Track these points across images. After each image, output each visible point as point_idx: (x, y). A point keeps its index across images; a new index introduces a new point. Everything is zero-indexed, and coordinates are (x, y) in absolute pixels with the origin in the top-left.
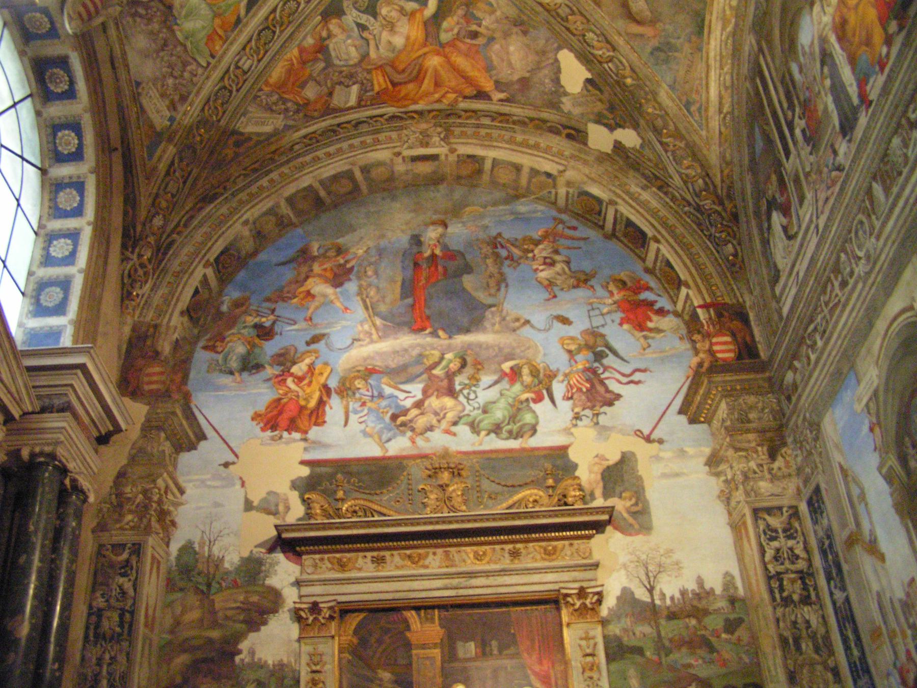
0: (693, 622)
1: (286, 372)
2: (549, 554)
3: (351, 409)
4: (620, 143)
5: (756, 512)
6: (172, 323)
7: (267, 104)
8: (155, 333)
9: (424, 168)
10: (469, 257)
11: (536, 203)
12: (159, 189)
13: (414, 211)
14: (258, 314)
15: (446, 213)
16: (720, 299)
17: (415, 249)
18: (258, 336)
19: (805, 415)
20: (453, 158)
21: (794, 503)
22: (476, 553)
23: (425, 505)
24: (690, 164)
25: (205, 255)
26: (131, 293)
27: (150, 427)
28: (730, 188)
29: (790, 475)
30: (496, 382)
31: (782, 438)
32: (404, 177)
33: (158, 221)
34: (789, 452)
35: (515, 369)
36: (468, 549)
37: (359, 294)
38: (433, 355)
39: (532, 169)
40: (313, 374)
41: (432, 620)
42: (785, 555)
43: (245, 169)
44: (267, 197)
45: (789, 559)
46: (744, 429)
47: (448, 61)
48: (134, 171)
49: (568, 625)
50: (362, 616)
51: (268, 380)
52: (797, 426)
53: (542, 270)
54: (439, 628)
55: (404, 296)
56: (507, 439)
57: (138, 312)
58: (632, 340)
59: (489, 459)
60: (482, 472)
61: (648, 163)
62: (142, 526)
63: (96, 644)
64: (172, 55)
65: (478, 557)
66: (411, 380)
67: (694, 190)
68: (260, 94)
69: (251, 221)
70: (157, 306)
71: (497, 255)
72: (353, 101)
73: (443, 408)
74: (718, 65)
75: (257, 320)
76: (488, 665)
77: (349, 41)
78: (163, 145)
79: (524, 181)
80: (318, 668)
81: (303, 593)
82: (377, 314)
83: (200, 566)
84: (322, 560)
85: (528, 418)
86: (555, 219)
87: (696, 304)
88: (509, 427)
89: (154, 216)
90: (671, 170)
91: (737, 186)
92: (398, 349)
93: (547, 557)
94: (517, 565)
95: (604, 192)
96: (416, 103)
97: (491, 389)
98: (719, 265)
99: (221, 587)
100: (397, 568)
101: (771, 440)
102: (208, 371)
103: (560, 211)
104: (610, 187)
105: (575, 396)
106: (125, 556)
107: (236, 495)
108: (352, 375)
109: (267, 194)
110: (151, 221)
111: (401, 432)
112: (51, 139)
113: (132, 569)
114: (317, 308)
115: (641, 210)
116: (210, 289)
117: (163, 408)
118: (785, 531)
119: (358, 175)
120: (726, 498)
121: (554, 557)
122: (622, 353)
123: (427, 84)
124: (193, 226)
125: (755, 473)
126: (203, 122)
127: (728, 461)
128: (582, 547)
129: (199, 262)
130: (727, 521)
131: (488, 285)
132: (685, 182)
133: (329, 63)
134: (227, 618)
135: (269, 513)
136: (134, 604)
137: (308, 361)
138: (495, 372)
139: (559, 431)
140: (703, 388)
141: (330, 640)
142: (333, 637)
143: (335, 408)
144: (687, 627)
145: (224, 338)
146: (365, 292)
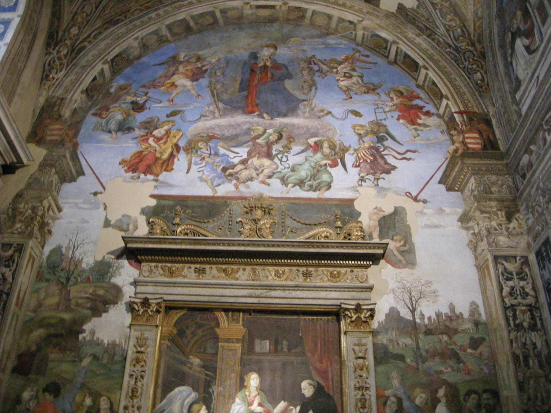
0: (446, 338)
1: (150, 134)
2: (334, 277)
3: (193, 161)
4: (403, 5)
5: (496, 258)
6: (75, 97)
8: (61, 103)
12: (78, 9)
13: (254, 38)
14: (135, 95)
16: (470, 109)
17: (253, 61)
18: (133, 109)
19: (538, 185)
20: (285, 8)
21: (525, 254)
22: (277, 271)
23: (240, 233)
24: (452, 18)
25: (105, 56)
26: (49, 76)
27: (44, 165)
28: (480, 35)
29: (522, 233)
30: (303, 151)
31: (516, 206)
33: (74, 31)
34: (521, 217)
35: (318, 143)
36: (271, 268)
37: (209, 86)
38: (258, 129)
40: (168, 137)
41: (238, 322)
42: (518, 292)
43: (141, 6)
44: (154, 24)
45: (521, 295)
46: (488, 198)
49: (345, 333)
50: (182, 313)
51: (136, 138)
52: (530, 196)
53: (342, 81)
54: (242, 327)
55: (241, 90)
56: (308, 191)
57: (52, 90)
58: (406, 130)
59: (293, 204)
60: (287, 213)
61: (422, 18)
62: (27, 232)
65: (277, 275)
66: (240, 145)
67: (454, 36)
69: (140, 37)
71: (311, 69)
75: (134, 99)
76: (279, 359)
79: (333, 24)
80: (142, 349)
81: (138, 291)
83: (64, 265)
84: (156, 267)
85: (325, 177)
86: (354, 49)
87: (453, 111)
88: (310, 183)
89: (72, 27)
90: (438, 23)
91: (486, 33)
93: (332, 279)
94: (308, 283)
95: (389, 35)
97: (299, 155)
98: (471, 88)
99: (77, 281)
100: (214, 277)
101: (508, 207)
103: (358, 45)
105: (361, 165)
106: (10, 252)
108: (197, 139)
109: (153, 22)
111: (228, 180)
113: (13, 262)
114: (178, 94)
115: (416, 49)
116: (104, 78)
118: (518, 274)
119: (218, 14)
120: (474, 248)
121: (338, 279)
122: (398, 138)
125: (496, 230)
127: (475, 220)
128: (360, 274)
130: (474, 263)
131: (303, 87)
132: (448, 31)
134: (78, 305)
135: (121, 229)
136: (10, 288)
137: (166, 127)
138: (303, 144)
139: (348, 189)
140: (458, 166)
141: (155, 329)
143: (181, 161)
144: (440, 341)
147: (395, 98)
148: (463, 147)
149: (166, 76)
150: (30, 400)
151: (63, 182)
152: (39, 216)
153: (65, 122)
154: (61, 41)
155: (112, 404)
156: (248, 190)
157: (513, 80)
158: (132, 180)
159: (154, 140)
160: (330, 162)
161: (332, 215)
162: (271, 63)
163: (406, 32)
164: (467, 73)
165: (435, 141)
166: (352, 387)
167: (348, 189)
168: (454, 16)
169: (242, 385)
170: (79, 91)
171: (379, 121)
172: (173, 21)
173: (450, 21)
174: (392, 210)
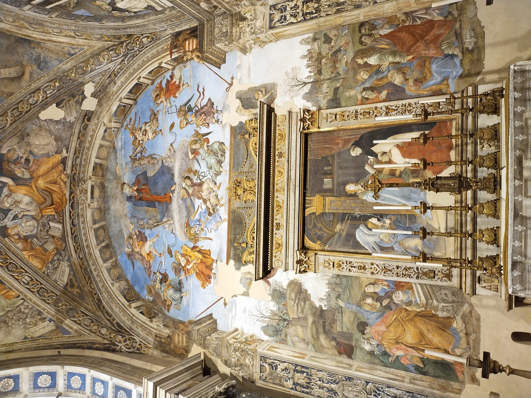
3: (204, 236)
5: (271, 28)
7: (53, 270)
12: (87, 329)
13: (116, 199)
18: (165, 282)
20: (93, 178)
24: (102, 57)
28: (115, 38)
29: (255, 10)
30: (198, 162)
31: (236, 14)
33: (104, 331)
34: (243, 10)
39: (102, 139)
40: (186, 255)
41: (311, 200)
43: (87, 283)
44: (102, 273)
47: (42, 176)
48: (75, 342)
51: (187, 278)
55: (154, 206)
63: (312, 389)
64: (12, 319)
66: (193, 205)
67: (115, 57)
68: (46, 273)
71: (140, 159)
72: (60, 226)
73: (208, 189)
74: (47, 35)
75: (158, 283)
77: (23, 225)
78: (64, 326)
79: (107, 143)
80: (332, 264)
83: (275, 324)
85: (216, 146)
86: (125, 129)
89: (101, 333)
96: (65, 195)
102: (180, 310)
103: (122, 126)
106: (267, 366)
107: (241, 300)
110: (103, 335)
112: (42, 390)
114: (156, 250)
116: (142, 306)
117: (195, 336)
118: (282, 12)
119: (97, 226)
121: (284, 135)
123: (55, 188)
125: (252, 28)
126: (55, 304)
129: (128, 310)
131: (153, 164)
132: (111, 61)
133: (35, 236)
134: (302, 311)
135: (251, 283)
136: (292, 364)
138: (193, 162)
139: (224, 131)
142: (316, 254)
143: (203, 244)
147: (161, 100)
148: (195, 52)
149: (143, 260)
150: (371, 344)
153: (173, 332)
154: (111, 341)
155: (370, 284)
156: (224, 198)
157: (147, 12)
160: (206, 143)
165: (191, 71)
166: (356, 121)
167: (224, 131)
169: (354, 195)
170: (150, 324)
172: (100, 259)
174: (238, 100)
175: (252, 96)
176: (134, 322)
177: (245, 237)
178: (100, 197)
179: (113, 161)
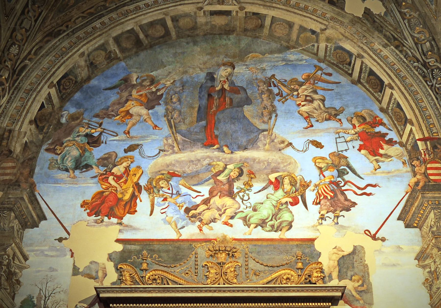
1: (109, 172)
3: (155, 202)
8: (9, 137)
9: (220, 21)
10: (249, 92)
11: (302, 53)
12: (16, 25)
13: (210, 54)
14: (89, 126)
15: (234, 57)
17: (209, 84)
18: (88, 143)
20: (241, 14)
23: (207, 277)
25: (50, 77)
30: (264, 189)
32: (204, 27)
33: (14, 50)
35: (279, 179)
38: (218, 165)
39: (301, 27)
40: (128, 175)
43: (83, 13)
44: (100, 35)
51: (95, 177)
55: (199, 119)
56: (269, 231)
59: (255, 245)
61: (389, 27)
70: (11, 115)
71: (271, 92)
75: (88, 131)
79: (294, 36)
82: (177, 132)
85: (286, 216)
86: (315, 66)
90: (406, 34)
92: (192, 159)
95: (354, 47)
97: (259, 193)
102: (49, 168)
103: (320, 61)
104: (359, 44)
105: (322, 202)
108: (158, 177)
109: (99, 33)
115: (381, 63)
116: (53, 105)
119: (169, 23)
122: (358, 172)
124: (41, 54)
129: (46, 83)
131: (262, 114)
132: (416, 44)
137: (125, 164)
138: (264, 181)
139: (308, 228)
145: (63, 144)
146: (170, 115)
147: (357, 125)
149: (119, 103)
151: (26, 228)
152: (4, 265)
158: (96, 224)
159: (114, 179)
160: (291, 200)
161: (294, 257)
162: (229, 86)
163: (372, 42)
164: (435, 93)
168: (423, 28)
171: (340, 153)
172: (120, 32)
173: (419, 33)
174: (351, 249)
175: (356, 270)
176: (28, 93)
177: (156, 267)
178: (213, 27)
179: (267, 47)
